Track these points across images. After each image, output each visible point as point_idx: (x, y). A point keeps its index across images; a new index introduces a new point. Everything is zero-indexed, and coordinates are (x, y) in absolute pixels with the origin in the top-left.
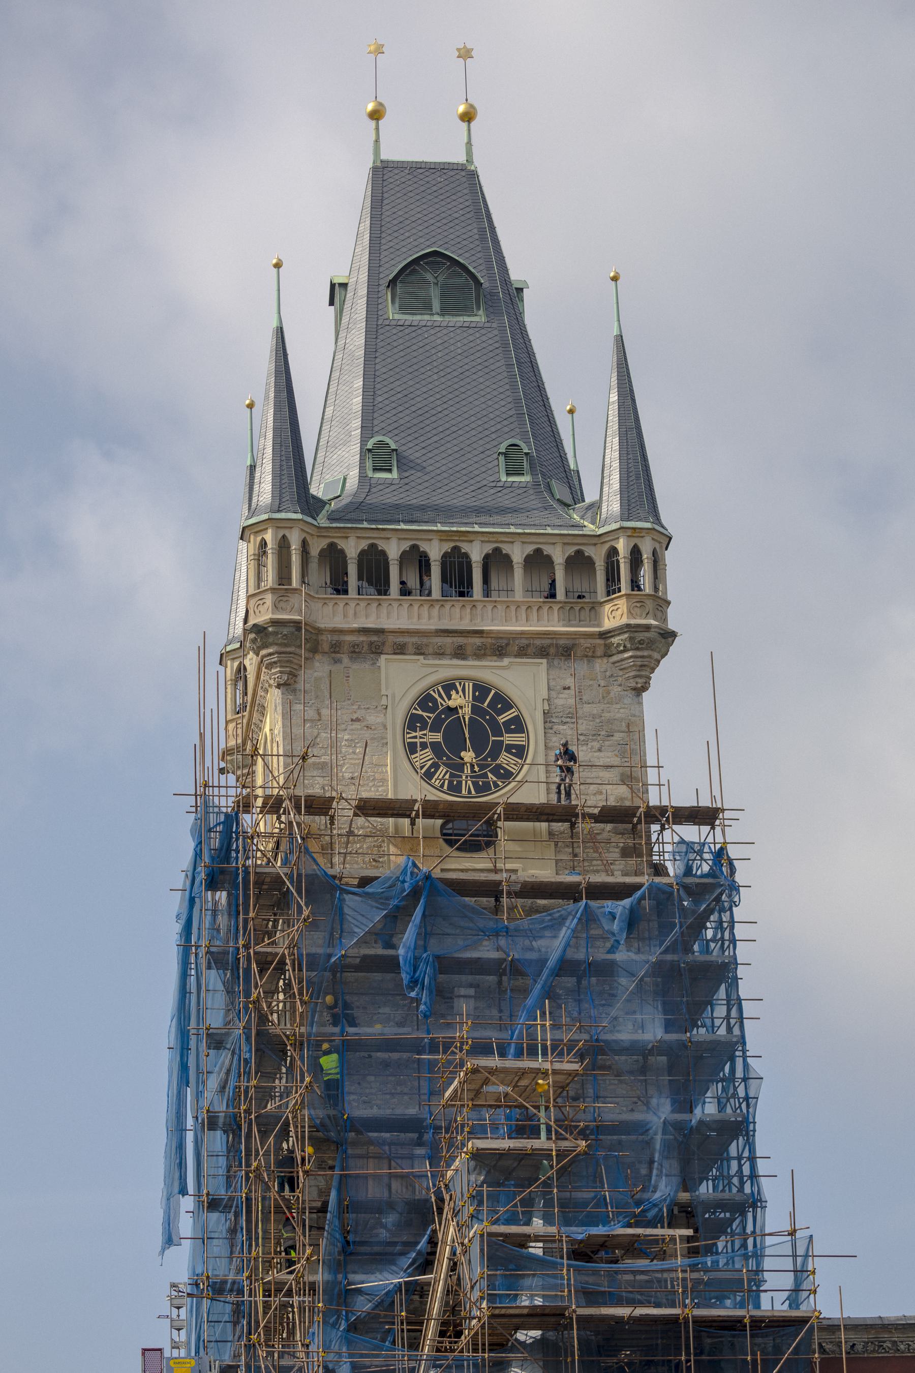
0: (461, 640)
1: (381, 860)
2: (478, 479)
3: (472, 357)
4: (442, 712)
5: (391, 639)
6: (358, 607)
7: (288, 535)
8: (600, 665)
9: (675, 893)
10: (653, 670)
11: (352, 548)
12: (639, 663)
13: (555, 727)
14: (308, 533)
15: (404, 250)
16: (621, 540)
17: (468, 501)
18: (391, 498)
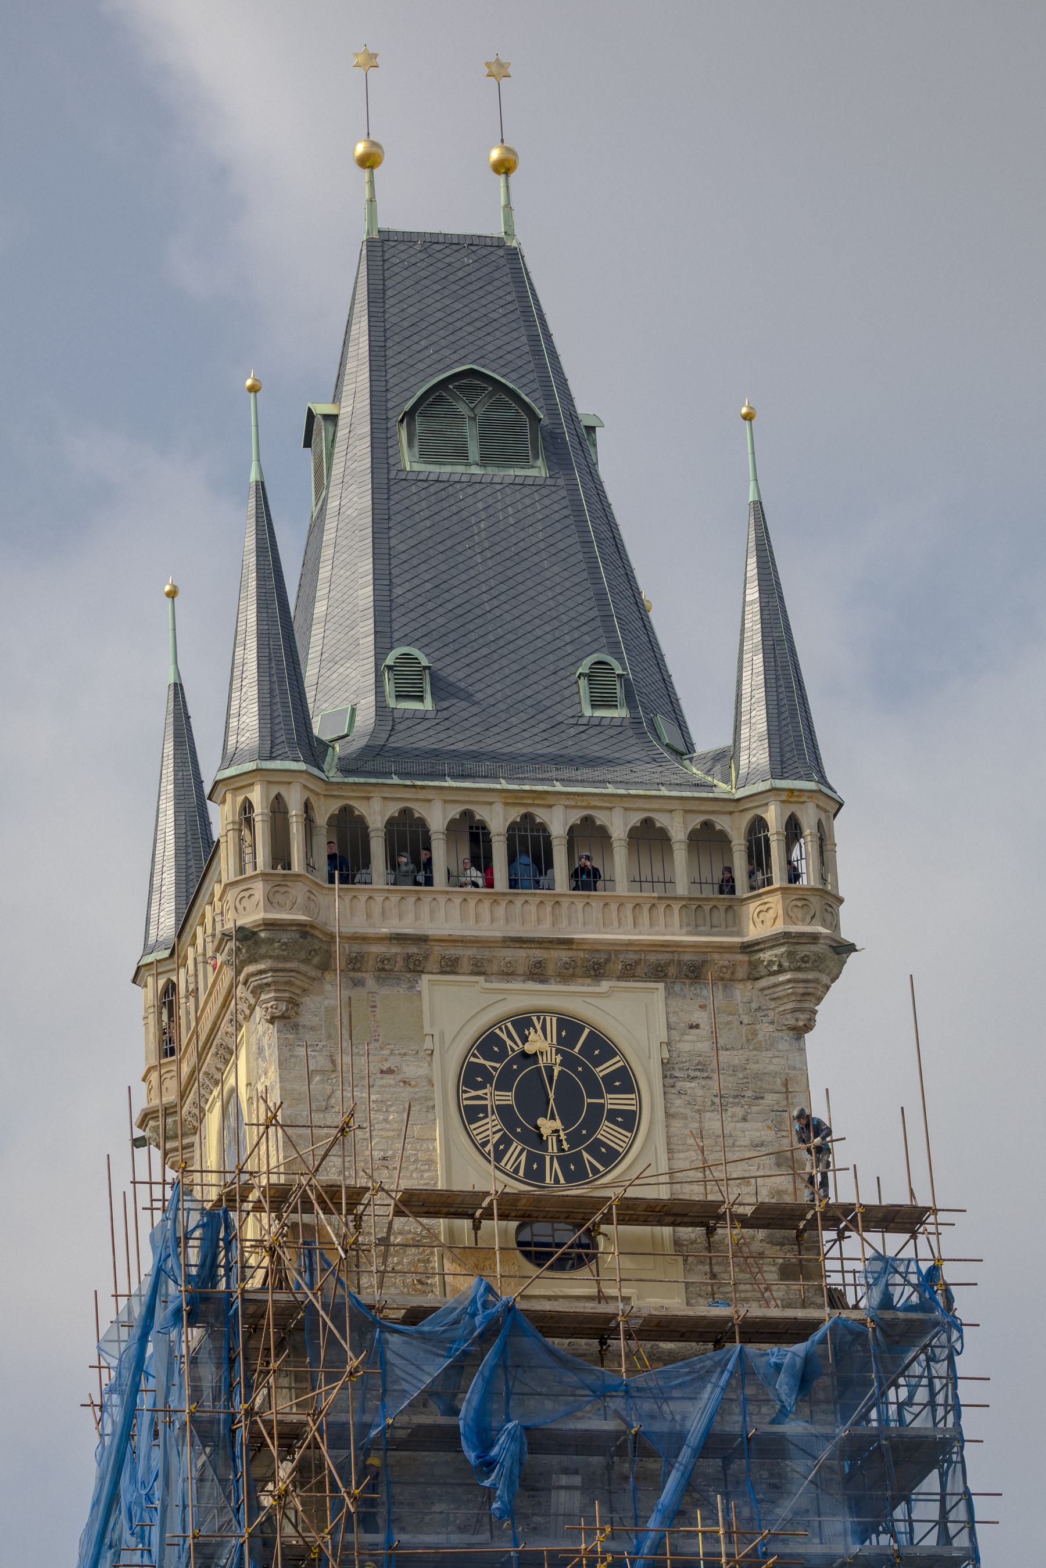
0: (538, 954)
1: (429, 1281)
2: (550, 712)
3: (531, 530)
4: (513, 1061)
5: (437, 950)
6: (387, 903)
7: (284, 793)
8: (742, 993)
9: (870, 1335)
10: (819, 999)
11: (376, 814)
12: (801, 991)
13: (679, 1084)
14: (312, 791)
15: (420, 366)
16: (772, 808)
17: (539, 746)
18: (424, 740)
